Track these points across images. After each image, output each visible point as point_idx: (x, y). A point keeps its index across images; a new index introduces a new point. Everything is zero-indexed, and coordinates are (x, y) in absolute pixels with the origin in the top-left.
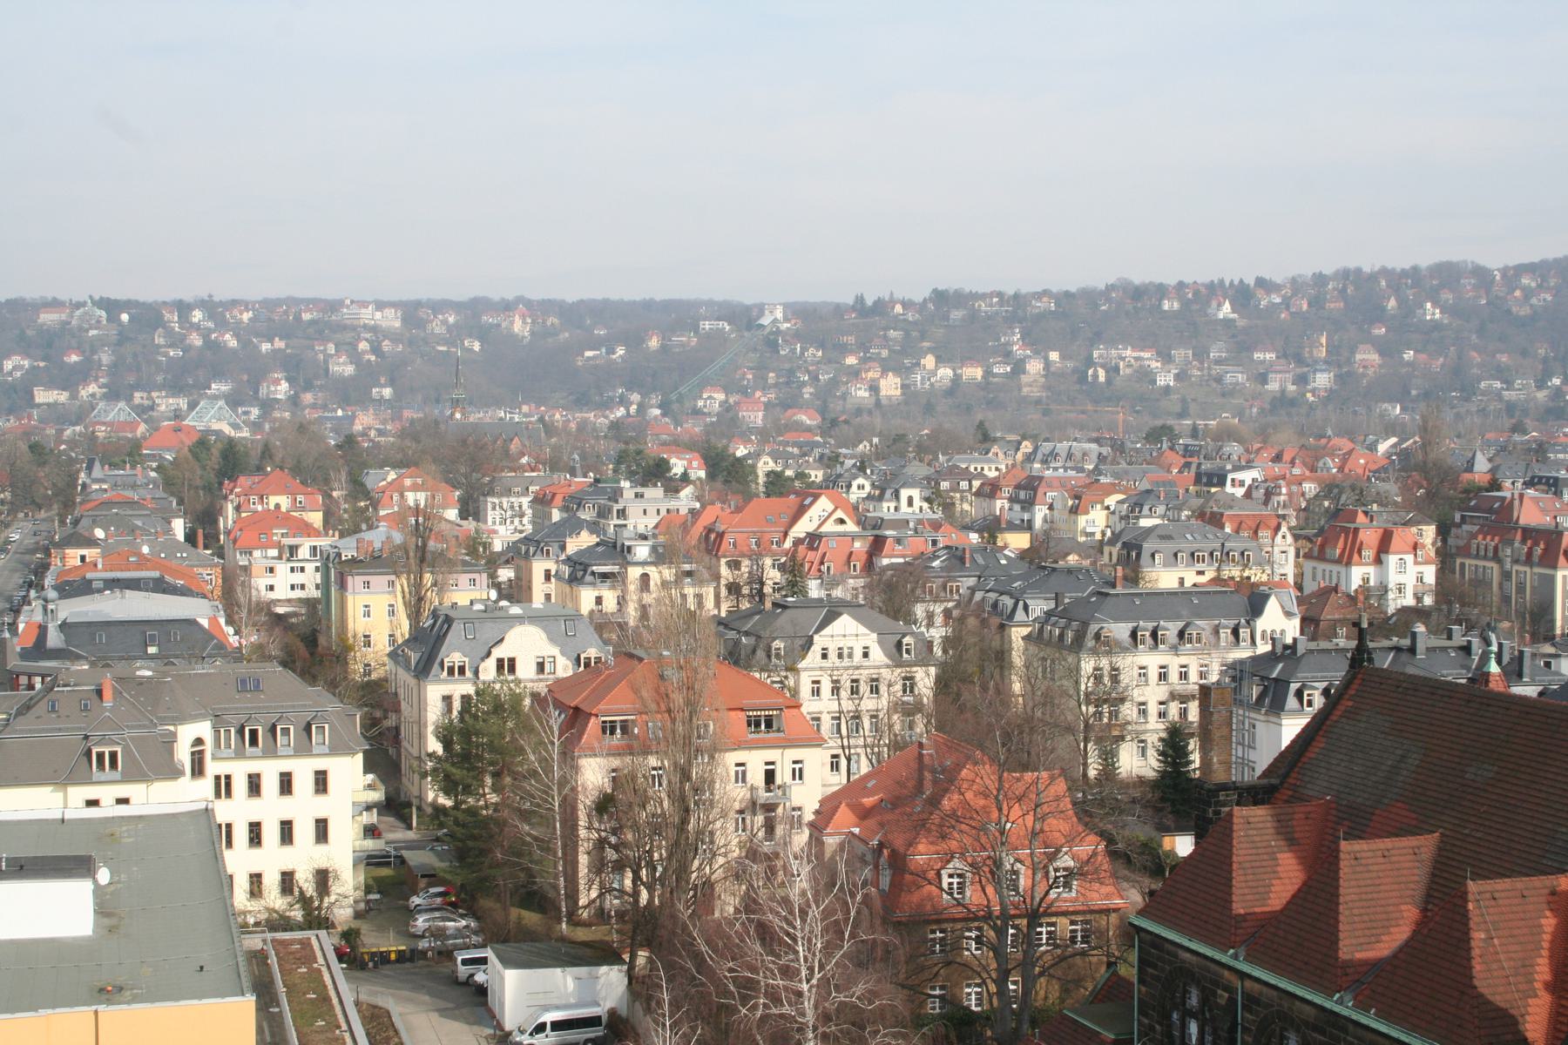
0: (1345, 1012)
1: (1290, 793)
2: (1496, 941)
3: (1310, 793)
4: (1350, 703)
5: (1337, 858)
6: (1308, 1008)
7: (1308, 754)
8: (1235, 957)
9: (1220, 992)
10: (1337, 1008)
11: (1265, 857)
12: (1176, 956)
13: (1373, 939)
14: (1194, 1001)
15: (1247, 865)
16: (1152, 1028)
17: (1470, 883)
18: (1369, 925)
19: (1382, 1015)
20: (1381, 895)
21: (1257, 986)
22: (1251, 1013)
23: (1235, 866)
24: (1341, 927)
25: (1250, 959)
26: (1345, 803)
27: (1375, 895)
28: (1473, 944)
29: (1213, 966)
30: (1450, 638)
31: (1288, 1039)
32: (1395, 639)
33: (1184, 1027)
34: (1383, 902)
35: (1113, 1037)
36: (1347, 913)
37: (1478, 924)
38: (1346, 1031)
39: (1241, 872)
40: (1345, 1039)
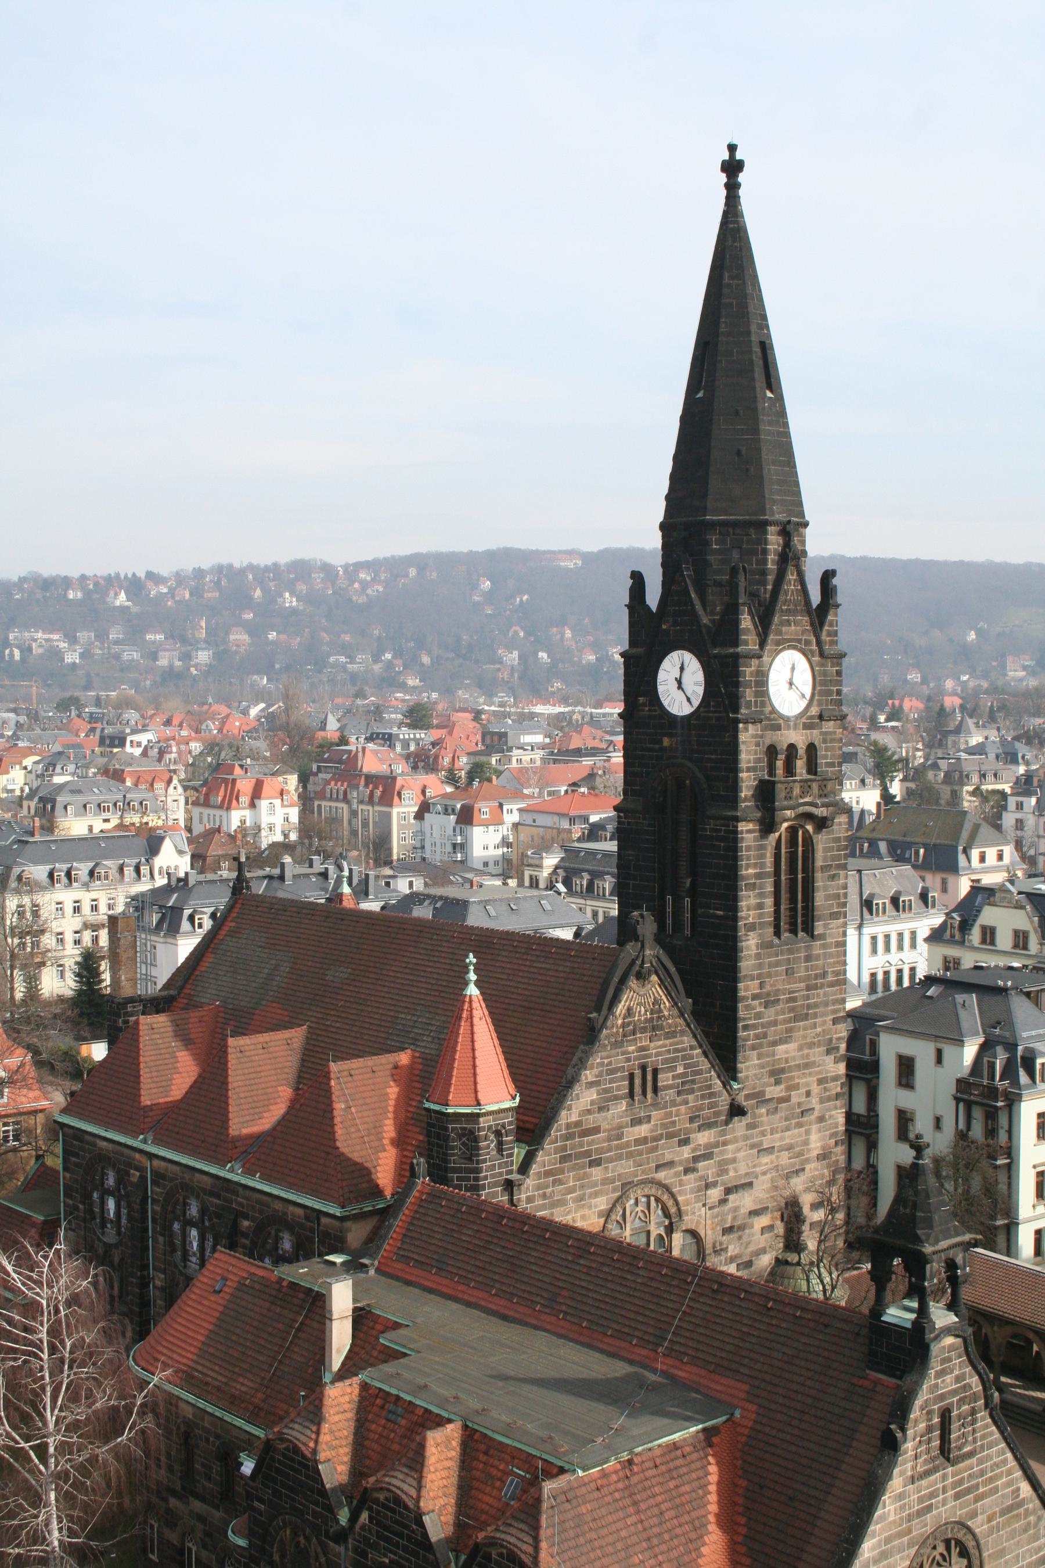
1: (186, 1001)
2: (353, 1110)
3: (203, 1000)
4: (233, 924)
5: (226, 1052)
6: (205, 1178)
7: (199, 968)
8: (145, 1141)
9: (132, 1171)
11: (167, 1056)
12: (95, 1145)
13: (256, 1117)
14: (111, 1181)
15: (152, 1064)
16: (77, 1208)
17: (332, 1064)
18: (253, 1105)
19: (266, 1178)
20: (262, 1080)
21: (163, 1164)
22: (159, 1186)
23: (142, 1065)
24: (231, 1109)
25: (156, 1142)
26: (231, 1006)
28: (335, 1113)
29: (126, 1151)
30: (311, 866)
31: (190, 1205)
32: (268, 869)
33: (103, 1203)
34: (264, 1086)
35: (42, 1218)
36: (235, 1097)
37: (338, 1097)
39: (147, 1070)
40: (236, 1201)
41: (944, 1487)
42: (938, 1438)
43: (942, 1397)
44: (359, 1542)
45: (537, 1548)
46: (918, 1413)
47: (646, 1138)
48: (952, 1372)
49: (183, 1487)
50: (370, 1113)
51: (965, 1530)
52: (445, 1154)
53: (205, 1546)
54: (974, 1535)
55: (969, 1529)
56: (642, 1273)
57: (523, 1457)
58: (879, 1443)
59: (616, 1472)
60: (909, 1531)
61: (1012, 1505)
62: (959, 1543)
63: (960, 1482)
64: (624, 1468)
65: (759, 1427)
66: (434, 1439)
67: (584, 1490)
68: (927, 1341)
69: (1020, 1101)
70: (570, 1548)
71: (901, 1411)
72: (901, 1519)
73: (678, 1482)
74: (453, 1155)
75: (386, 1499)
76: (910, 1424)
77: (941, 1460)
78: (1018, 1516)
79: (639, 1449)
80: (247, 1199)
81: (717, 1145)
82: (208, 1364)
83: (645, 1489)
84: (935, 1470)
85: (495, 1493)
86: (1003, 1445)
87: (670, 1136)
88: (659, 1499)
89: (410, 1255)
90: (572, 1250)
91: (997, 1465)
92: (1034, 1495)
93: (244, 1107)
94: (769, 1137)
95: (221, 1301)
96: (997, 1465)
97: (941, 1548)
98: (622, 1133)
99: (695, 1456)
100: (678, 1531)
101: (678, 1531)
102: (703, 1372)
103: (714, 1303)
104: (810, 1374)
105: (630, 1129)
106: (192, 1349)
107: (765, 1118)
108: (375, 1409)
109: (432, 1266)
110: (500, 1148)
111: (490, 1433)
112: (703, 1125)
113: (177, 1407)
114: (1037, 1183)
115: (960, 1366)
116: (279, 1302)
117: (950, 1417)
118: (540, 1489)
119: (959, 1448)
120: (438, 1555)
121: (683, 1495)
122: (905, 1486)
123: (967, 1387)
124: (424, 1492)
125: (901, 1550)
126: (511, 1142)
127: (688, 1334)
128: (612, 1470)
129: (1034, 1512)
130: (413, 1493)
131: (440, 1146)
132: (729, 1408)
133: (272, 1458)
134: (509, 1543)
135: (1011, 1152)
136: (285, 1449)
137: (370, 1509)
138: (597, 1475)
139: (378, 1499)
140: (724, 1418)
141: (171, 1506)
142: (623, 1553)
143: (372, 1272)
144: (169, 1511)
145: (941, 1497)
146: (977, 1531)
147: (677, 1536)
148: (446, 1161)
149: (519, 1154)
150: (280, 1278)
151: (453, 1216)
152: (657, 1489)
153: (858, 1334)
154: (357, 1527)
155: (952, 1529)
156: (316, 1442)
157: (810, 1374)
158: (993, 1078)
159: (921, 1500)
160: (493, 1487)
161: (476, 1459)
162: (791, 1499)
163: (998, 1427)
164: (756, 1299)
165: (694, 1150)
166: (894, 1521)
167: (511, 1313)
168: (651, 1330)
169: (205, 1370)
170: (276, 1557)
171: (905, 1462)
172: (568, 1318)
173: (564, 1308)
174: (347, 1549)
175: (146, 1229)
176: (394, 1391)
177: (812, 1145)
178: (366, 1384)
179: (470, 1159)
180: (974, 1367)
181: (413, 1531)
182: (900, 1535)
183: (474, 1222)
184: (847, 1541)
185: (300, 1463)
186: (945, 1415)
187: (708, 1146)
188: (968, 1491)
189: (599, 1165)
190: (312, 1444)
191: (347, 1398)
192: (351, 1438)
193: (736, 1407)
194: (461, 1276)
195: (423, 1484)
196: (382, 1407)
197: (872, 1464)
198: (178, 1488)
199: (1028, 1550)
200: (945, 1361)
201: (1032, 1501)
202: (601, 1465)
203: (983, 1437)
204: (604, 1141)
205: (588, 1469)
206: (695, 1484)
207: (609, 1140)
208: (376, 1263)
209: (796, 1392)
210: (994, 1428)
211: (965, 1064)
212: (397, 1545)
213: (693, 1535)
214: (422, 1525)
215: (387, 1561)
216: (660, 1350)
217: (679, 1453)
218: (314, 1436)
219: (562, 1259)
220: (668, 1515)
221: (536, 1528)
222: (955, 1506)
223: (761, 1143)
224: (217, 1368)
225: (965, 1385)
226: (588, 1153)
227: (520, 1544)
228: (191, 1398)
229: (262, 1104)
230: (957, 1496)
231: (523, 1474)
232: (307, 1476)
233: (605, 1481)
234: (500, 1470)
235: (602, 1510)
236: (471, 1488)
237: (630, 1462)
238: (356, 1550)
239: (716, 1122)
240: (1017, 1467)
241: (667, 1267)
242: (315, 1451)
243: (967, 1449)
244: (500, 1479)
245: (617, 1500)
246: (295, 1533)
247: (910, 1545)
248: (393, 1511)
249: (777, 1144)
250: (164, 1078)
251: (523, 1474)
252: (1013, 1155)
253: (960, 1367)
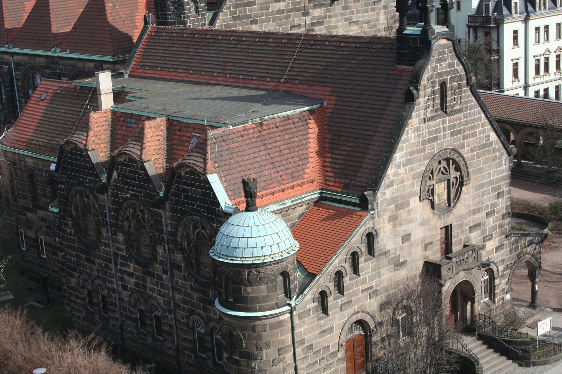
0: (57, 55)
2: (117, 7)
9: (4, 66)
10: (53, 54)
11: (19, 4)
13: (67, 24)
15: (10, 8)
18: (65, 18)
19: (72, 51)
20: (70, 5)
21: (19, 57)
23: (4, 8)
24: (52, 20)
27: (66, 6)
28: (107, 8)
31: (35, 78)
34: (71, 8)
36: (54, 13)
38: (58, 64)
39: (7, 11)
40: (58, 67)
41: (444, 127)
42: (439, 98)
43: (440, 75)
44: (114, 190)
45: (205, 164)
46: (426, 82)
47: (283, 10)
48: (446, 61)
49: (33, 206)
50: (127, 9)
51: (457, 154)
52: (166, 14)
53: (48, 234)
54: (463, 158)
55: (460, 154)
56: (272, 44)
57: (199, 127)
58: (403, 101)
59: (253, 128)
60: (424, 150)
61: (485, 144)
62: (454, 162)
63: (454, 126)
64: (257, 127)
65: (337, 107)
66: (149, 125)
67: (233, 136)
68: (429, 39)
69: (504, 23)
70: (226, 165)
71: (416, 80)
72: (419, 142)
73: (291, 136)
74: (170, 14)
75: (125, 160)
76: (421, 88)
77: (440, 112)
78: (489, 151)
79: (266, 118)
80: (64, 65)
81: (325, 17)
82: (39, 136)
83: (270, 138)
84: (438, 117)
85: (185, 149)
86: (479, 109)
87: (297, 10)
88: (279, 143)
89: (147, 64)
90: (233, 42)
91: (476, 120)
92: (499, 140)
93: (60, 19)
94: (355, 15)
95: (45, 104)
96: (476, 120)
97: (444, 164)
98: (269, 6)
99: (300, 124)
100: (291, 160)
101: (291, 160)
102: (306, 87)
103: (311, 51)
104: (364, 75)
105: (274, 4)
106: (31, 131)
107: (352, 4)
108: (120, 123)
109: (158, 67)
110: (197, 11)
111: (181, 120)
112: (316, 5)
113: (25, 161)
114: (514, 69)
115: (450, 58)
116: (75, 98)
117: (446, 87)
118: (206, 134)
119: (453, 107)
120: (154, 183)
121: (294, 142)
122: (420, 124)
123: (456, 71)
124: (144, 151)
125: (419, 160)
126: (203, 7)
127: (297, 70)
128: (250, 127)
129: (499, 150)
130: (139, 152)
131: (162, 11)
132: (320, 101)
133: (65, 157)
134: (190, 163)
135: (499, 52)
136: (72, 149)
137: (117, 169)
138: (241, 129)
139: (121, 162)
140: (318, 106)
141: (29, 217)
142: (258, 169)
143: (126, 76)
144: (28, 221)
145: (442, 133)
146: (465, 156)
147: (290, 163)
148: (166, 18)
149: (209, 15)
150: (75, 85)
151: (169, 40)
152: (278, 139)
153: (391, 49)
154: (112, 181)
155: (450, 153)
156: (86, 141)
157: (364, 75)
158: (488, 12)
159: (430, 133)
160: (184, 146)
161: (175, 135)
162: (355, 138)
163: (475, 97)
164: (335, 44)
165: (312, 19)
166: (414, 143)
167: (202, 81)
168: (277, 72)
169: (38, 139)
170: (74, 213)
171: (419, 110)
172: (232, 76)
173: (229, 72)
174: (108, 196)
175: (14, 96)
176: (130, 112)
177: (381, 22)
178: (115, 111)
179: (180, 17)
180: (460, 60)
181: (140, 174)
182: (418, 152)
183: (180, 40)
184: (387, 152)
185: (80, 155)
186: (443, 85)
187: (320, 17)
188: (459, 132)
189: (256, 23)
190: (84, 142)
191: (104, 119)
192: (108, 139)
193: (324, 100)
194: (174, 68)
195: (144, 147)
196: (124, 121)
197: (400, 112)
198: (31, 206)
199: (496, 171)
200: (440, 53)
201: (497, 144)
202: (244, 123)
203: (467, 102)
204: (259, 10)
205: (235, 126)
206: (301, 138)
207: (261, 9)
208: (128, 72)
209: (358, 85)
210: (473, 98)
211: (473, 7)
212: (133, 185)
213: (300, 163)
214: (144, 169)
215: (129, 196)
216: (282, 81)
217: (291, 121)
218: (85, 138)
219: (228, 47)
220: (285, 152)
221: (205, 154)
222: (451, 140)
223: (351, 18)
224: (44, 137)
225: (454, 70)
226: (249, 17)
227: (196, 163)
228: (31, 154)
229: (70, 18)
230: (452, 134)
231: (199, 135)
232: (84, 161)
233: (245, 133)
234: (187, 137)
235: (245, 147)
236: (172, 149)
237: (261, 124)
238: (113, 196)
239: (324, 4)
240: (488, 123)
241: (285, 39)
242: (85, 145)
243: (457, 107)
244: (187, 142)
245: (253, 142)
246: (82, 197)
247: (425, 158)
248: (129, 166)
249: (360, 20)
250: (18, 15)
251: (199, 135)
252: (500, 54)
253: (451, 58)
